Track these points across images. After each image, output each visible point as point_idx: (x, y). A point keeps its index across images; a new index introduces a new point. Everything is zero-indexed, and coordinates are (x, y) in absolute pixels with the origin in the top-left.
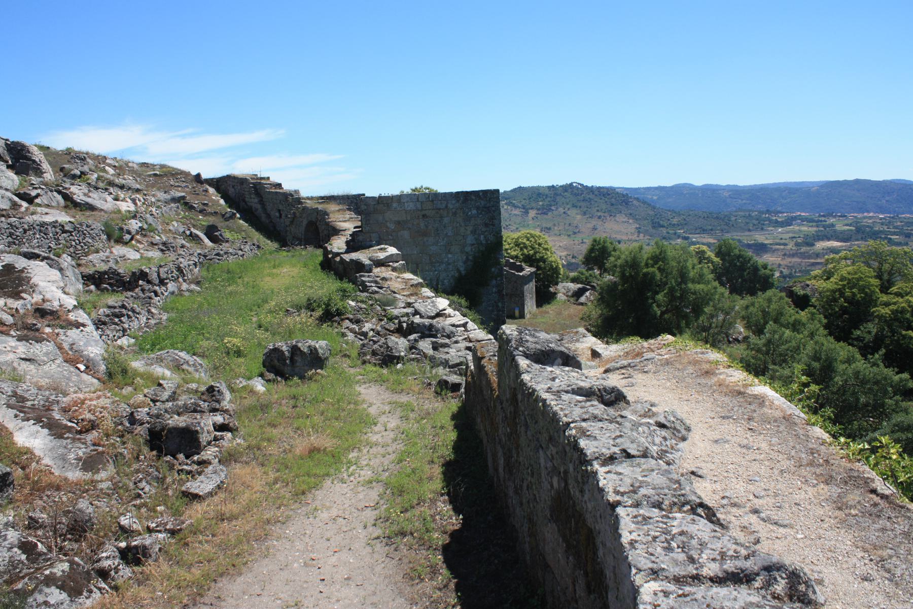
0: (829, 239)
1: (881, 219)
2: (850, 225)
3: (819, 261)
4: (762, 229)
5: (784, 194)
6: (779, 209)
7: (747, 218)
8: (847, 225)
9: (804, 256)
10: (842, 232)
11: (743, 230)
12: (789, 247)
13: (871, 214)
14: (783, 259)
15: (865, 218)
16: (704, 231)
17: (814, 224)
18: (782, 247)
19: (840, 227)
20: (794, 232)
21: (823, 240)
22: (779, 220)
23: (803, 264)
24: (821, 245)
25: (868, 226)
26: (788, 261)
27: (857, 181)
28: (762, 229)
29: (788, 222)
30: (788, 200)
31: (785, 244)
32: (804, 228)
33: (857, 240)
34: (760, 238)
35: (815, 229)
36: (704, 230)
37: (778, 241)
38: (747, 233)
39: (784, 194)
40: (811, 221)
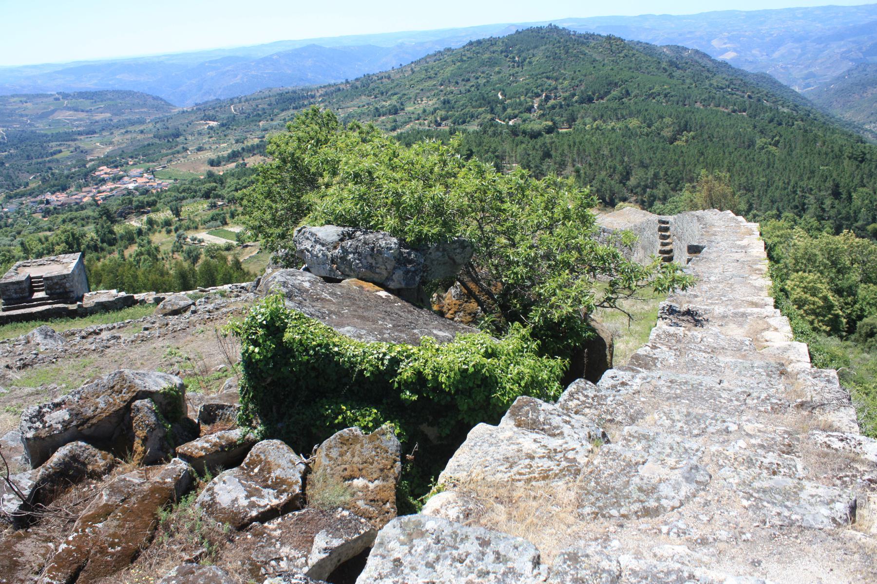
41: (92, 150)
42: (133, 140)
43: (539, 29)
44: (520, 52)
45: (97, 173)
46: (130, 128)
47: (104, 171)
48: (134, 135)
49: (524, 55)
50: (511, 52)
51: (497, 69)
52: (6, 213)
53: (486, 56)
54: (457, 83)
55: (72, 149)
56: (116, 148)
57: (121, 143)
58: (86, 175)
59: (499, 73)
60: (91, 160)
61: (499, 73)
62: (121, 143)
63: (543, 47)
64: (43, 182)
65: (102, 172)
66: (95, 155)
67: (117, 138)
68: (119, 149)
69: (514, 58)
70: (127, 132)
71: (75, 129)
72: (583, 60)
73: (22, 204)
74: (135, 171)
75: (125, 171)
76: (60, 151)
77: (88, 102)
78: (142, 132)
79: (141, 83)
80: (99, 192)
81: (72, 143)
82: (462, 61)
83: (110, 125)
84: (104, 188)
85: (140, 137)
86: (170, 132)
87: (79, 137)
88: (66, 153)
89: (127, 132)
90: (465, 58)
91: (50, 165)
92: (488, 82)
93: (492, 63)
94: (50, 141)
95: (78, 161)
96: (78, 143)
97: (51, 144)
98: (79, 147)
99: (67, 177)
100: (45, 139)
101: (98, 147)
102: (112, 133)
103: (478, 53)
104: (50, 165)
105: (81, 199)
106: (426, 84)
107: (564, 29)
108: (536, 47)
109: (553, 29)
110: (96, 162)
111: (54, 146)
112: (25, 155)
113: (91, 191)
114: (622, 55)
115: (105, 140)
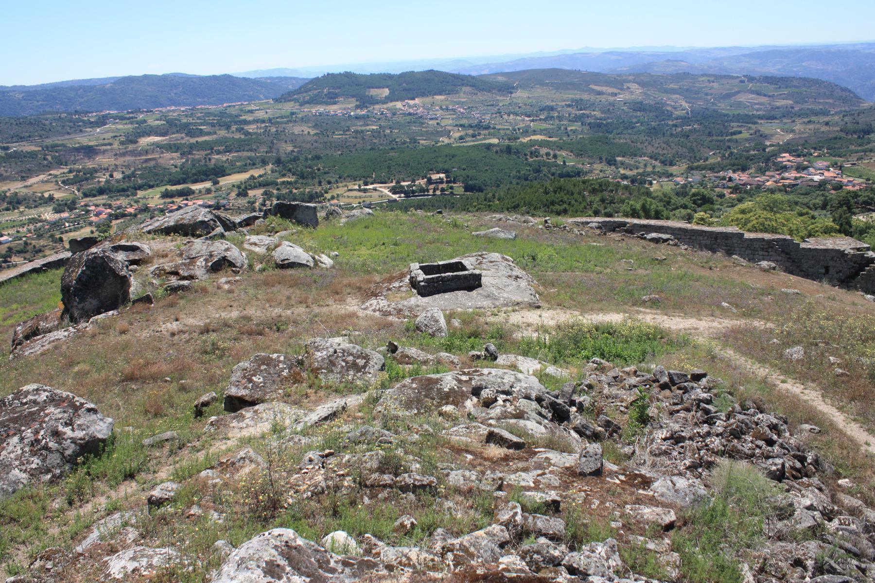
0: (149, 135)
1: (183, 111)
2: (161, 120)
3: (150, 157)
4: (81, 131)
5: (79, 92)
6: (78, 108)
7: (58, 120)
8: (157, 120)
9: (133, 153)
10: (158, 127)
11: (63, 134)
12: (116, 146)
13: (173, 108)
14: (116, 159)
15: (169, 111)
16: (21, 139)
17: (128, 121)
18: (109, 147)
19: (153, 122)
20: (113, 131)
21: (143, 136)
22: (92, 120)
23: (137, 162)
24: (145, 141)
25: (176, 119)
26: (120, 161)
27: (146, 77)
28: (81, 131)
29: (102, 121)
30: (86, 98)
31: (111, 144)
32: (120, 127)
33: (173, 133)
34: (83, 140)
35: (130, 126)
36: (21, 138)
37: (102, 142)
38: (67, 137)
39: (79, 92)
40: (122, 118)
41: (772, 135)
42: (816, 132)
45: (779, 159)
46: (813, 118)
47: (786, 158)
48: (818, 126)
52: (690, 182)
55: (752, 132)
56: (797, 136)
57: (803, 133)
58: (767, 160)
60: (771, 145)
62: (803, 133)
64: (722, 160)
65: (784, 159)
66: (775, 141)
67: (798, 127)
68: (800, 138)
70: (810, 122)
71: (755, 112)
73: (705, 177)
74: (821, 164)
75: (809, 161)
76: (740, 132)
77: (771, 87)
78: (827, 124)
79: (812, 69)
80: (783, 179)
81: (753, 126)
83: (791, 112)
84: (786, 175)
85: (824, 129)
86: (860, 127)
87: (760, 121)
88: (745, 135)
89: (810, 122)
91: (729, 144)
94: (731, 121)
95: (756, 145)
96: (759, 127)
97: (732, 124)
98: (759, 131)
99: (747, 158)
100: (725, 119)
101: (778, 134)
102: (794, 121)
104: (729, 144)
105: (763, 182)
110: (776, 148)
111: (735, 126)
112: (707, 132)
113: (773, 176)
115: (786, 127)
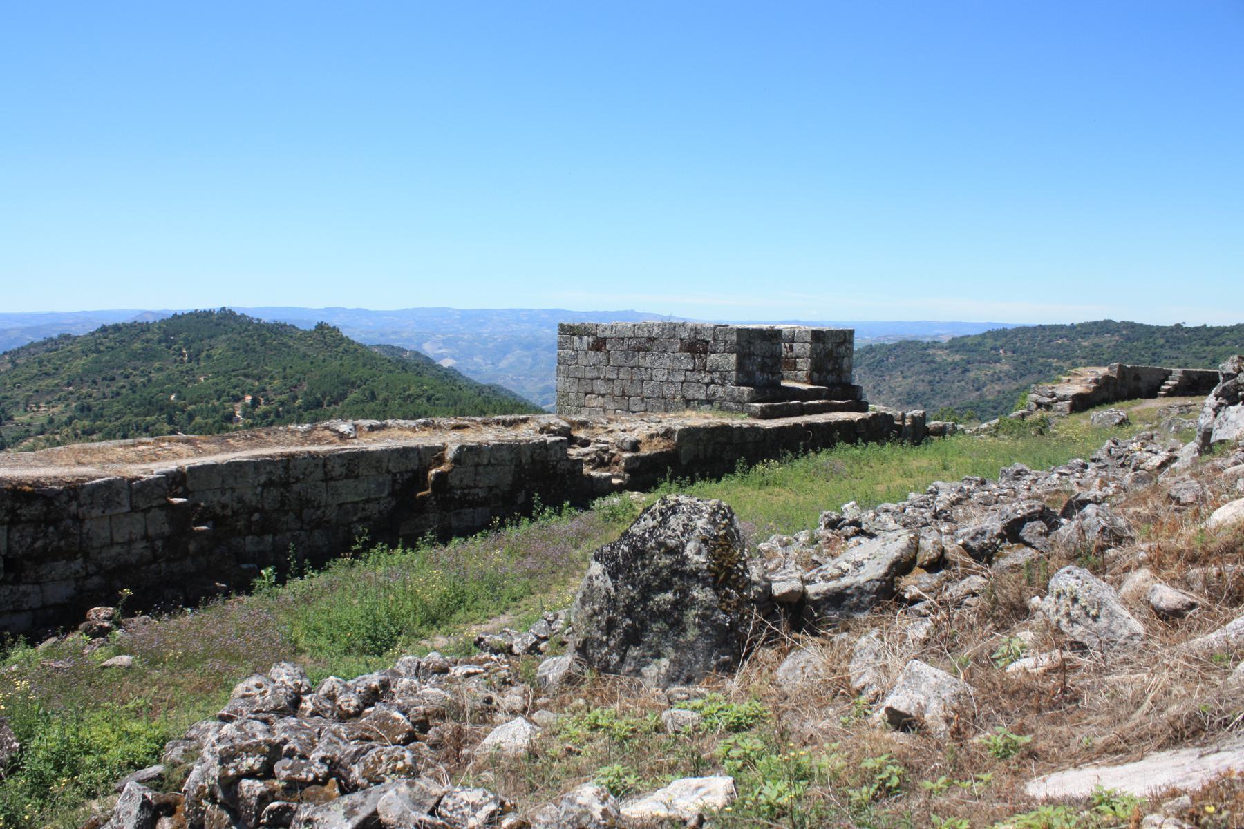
43: (208, 314)
44: (188, 343)
49: (196, 346)
50: (175, 342)
51: (157, 364)
53: (137, 346)
54: (95, 382)
59: (161, 369)
61: (161, 369)
63: (224, 337)
69: (180, 349)
72: (288, 354)
82: (98, 351)
90: (102, 348)
92: (150, 380)
93: (148, 355)
103: (122, 341)
106: (41, 383)
107: (243, 315)
108: (211, 337)
109: (227, 316)
114: (340, 349)
